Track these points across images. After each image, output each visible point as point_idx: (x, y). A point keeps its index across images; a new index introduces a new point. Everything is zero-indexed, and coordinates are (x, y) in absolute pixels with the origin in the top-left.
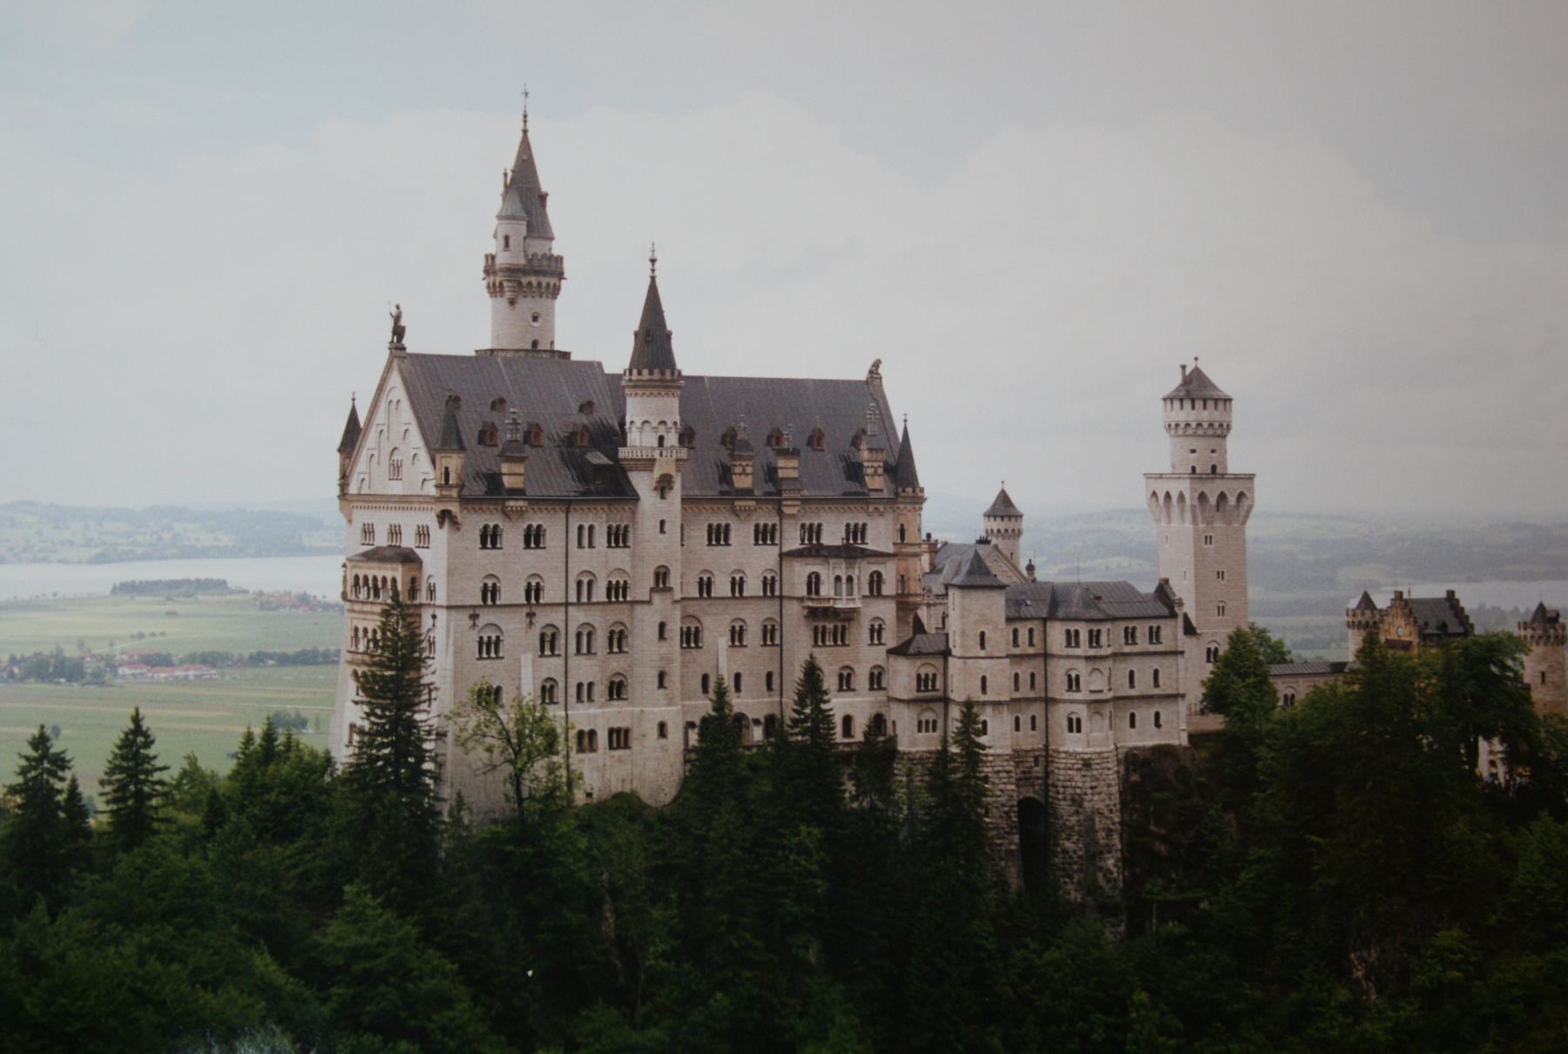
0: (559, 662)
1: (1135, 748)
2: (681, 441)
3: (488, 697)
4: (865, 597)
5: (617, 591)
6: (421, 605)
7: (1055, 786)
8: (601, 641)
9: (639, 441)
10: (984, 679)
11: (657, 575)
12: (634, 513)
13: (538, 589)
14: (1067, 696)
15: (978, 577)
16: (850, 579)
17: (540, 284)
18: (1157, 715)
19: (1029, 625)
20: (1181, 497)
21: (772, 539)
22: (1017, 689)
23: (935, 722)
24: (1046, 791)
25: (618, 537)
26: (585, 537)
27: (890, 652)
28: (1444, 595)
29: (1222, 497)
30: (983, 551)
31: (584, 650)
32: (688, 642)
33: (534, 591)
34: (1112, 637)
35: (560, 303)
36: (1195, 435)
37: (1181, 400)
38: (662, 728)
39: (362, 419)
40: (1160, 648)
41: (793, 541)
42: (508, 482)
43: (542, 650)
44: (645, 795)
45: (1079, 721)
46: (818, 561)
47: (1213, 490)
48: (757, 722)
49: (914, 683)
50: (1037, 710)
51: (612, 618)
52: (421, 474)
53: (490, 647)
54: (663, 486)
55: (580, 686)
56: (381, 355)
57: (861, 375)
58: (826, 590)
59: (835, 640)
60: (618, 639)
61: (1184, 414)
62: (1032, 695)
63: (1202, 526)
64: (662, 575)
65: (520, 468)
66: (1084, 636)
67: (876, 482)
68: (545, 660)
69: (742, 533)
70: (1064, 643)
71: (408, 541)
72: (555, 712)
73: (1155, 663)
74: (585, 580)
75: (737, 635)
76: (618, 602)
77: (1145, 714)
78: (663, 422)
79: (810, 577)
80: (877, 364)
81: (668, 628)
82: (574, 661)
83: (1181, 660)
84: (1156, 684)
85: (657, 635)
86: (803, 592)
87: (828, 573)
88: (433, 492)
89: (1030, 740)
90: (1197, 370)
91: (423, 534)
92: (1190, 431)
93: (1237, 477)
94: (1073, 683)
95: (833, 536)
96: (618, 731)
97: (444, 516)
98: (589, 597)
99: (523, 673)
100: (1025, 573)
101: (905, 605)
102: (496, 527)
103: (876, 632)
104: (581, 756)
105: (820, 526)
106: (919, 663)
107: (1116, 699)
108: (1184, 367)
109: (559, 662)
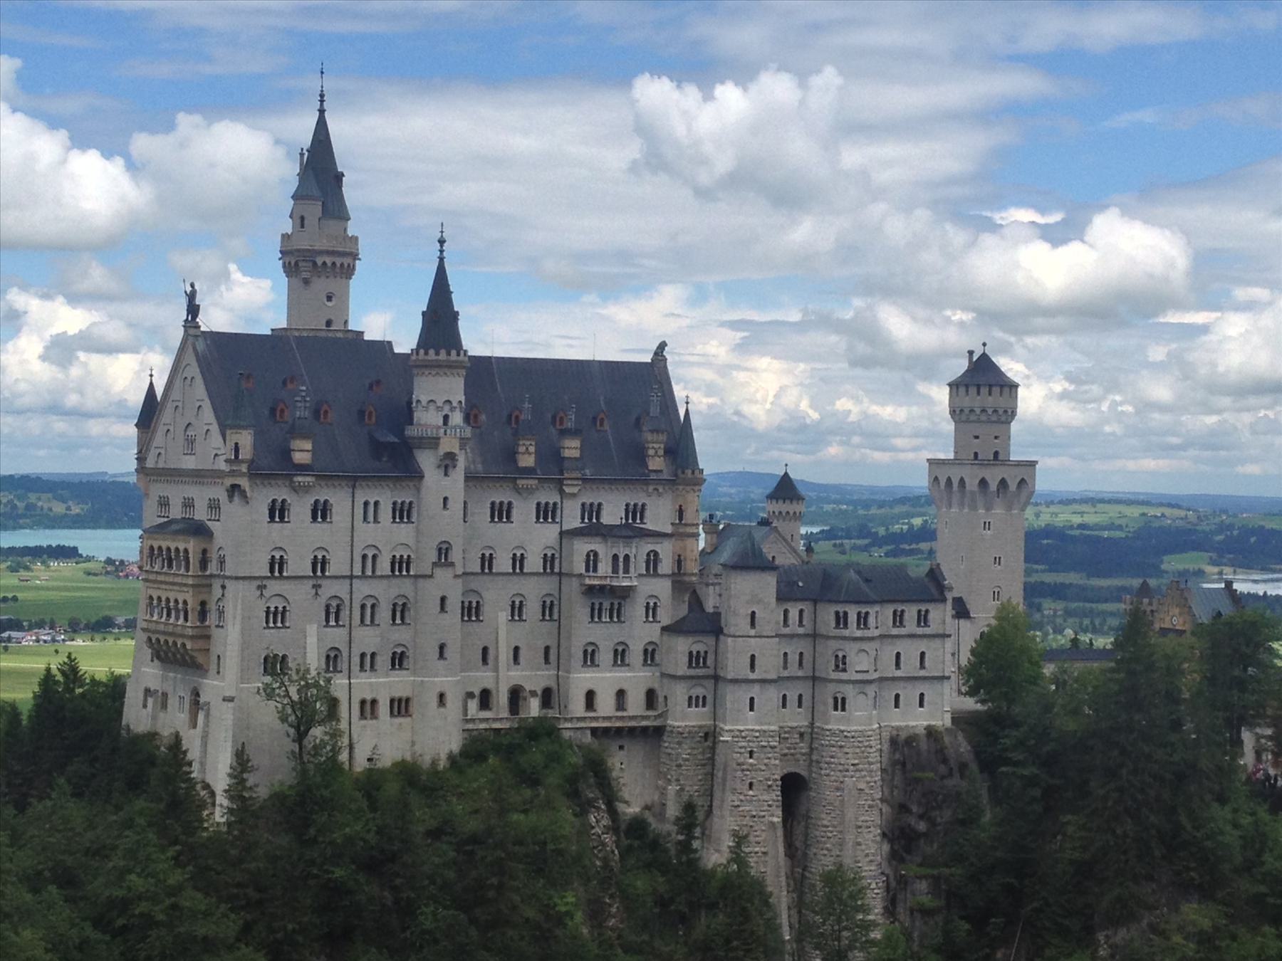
0: (343, 632)
1: (898, 729)
2: (467, 419)
3: (274, 665)
4: (641, 575)
5: (400, 565)
6: (211, 576)
7: (818, 762)
8: (384, 614)
9: (427, 419)
10: (753, 657)
11: (440, 549)
12: (418, 490)
14: (834, 676)
15: (751, 562)
16: (627, 557)
17: (334, 264)
18: (922, 695)
19: (800, 606)
20: (962, 481)
21: (553, 518)
22: (785, 667)
23: (704, 698)
24: (810, 765)
25: (402, 513)
26: (371, 512)
27: (664, 629)
28: (1223, 585)
29: (1003, 483)
30: (759, 533)
31: (368, 621)
32: (470, 616)
33: (320, 564)
34: (881, 616)
35: (354, 282)
36: (979, 421)
37: (967, 386)
38: (442, 696)
39: (159, 391)
40: (927, 631)
41: (573, 520)
42: (299, 457)
43: (327, 620)
44: (426, 761)
45: (844, 700)
46: (598, 539)
47: (993, 476)
48: (533, 693)
49: (686, 659)
50: (804, 689)
51: (394, 592)
52: (213, 448)
53: (276, 616)
54: (447, 463)
55: (363, 655)
56: (178, 334)
57: (647, 358)
58: (604, 567)
59: (611, 617)
60: (400, 611)
61: (971, 400)
62: (800, 674)
63: (982, 511)
64: (444, 551)
65: (308, 446)
66: (852, 618)
67: (656, 463)
68: (329, 630)
69: (524, 510)
70: (833, 624)
71: (201, 514)
72: (340, 682)
73: (923, 645)
75: (517, 610)
76: (401, 575)
77: (909, 694)
78: (449, 402)
79: (588, 555)
80: (663, 346)
81: (448, 602)
82: (359, 633)
83: (949, 645)
84: (922, 666)
85: (439, 609)
86: (583, 571)
87: (604, 550)
88: (223, 466)
89: (796, 718)
90: (984, 358)
91: (214, 506)
92: (973, 418)
93: (1019, 464)
94: (841, 663)
95: (612, 515)
96: (400, 700)
97: (234, 490)
98: (373, 571)
99: (310, 644)
100: (804, 555)
101: (679, 582)
102: (284, 501)
103: (651, 610)
104: (363, 722)
105: (600, 505)
106: (691, 640)
107: (882, 679)
108: (971, 353)
109: (343, 632)
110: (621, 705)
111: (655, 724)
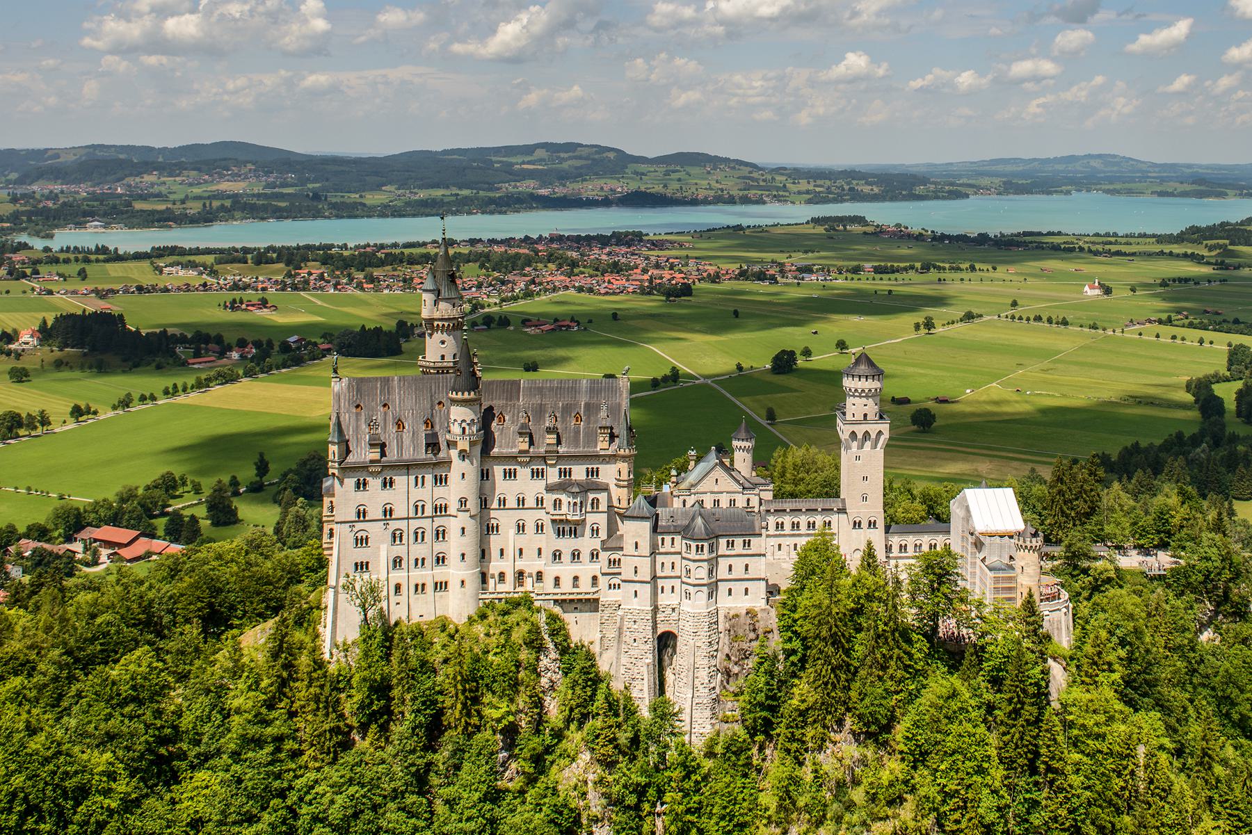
3: (362, 566)
13: (391, 510)
25: (440, 480)
29: (866, 435)
33: (388, 512)
47: (860, 430)
48: (530, 575)
51: (436, 525)
60: (440, 534)
72: (398, 576)
73: (746, 560)
74: (420, 504)
75: (521, 528)
77: (738, 588)
82: (413, 547)
103: (595, 532)
110: (576, 586)
111: (595, 596)
